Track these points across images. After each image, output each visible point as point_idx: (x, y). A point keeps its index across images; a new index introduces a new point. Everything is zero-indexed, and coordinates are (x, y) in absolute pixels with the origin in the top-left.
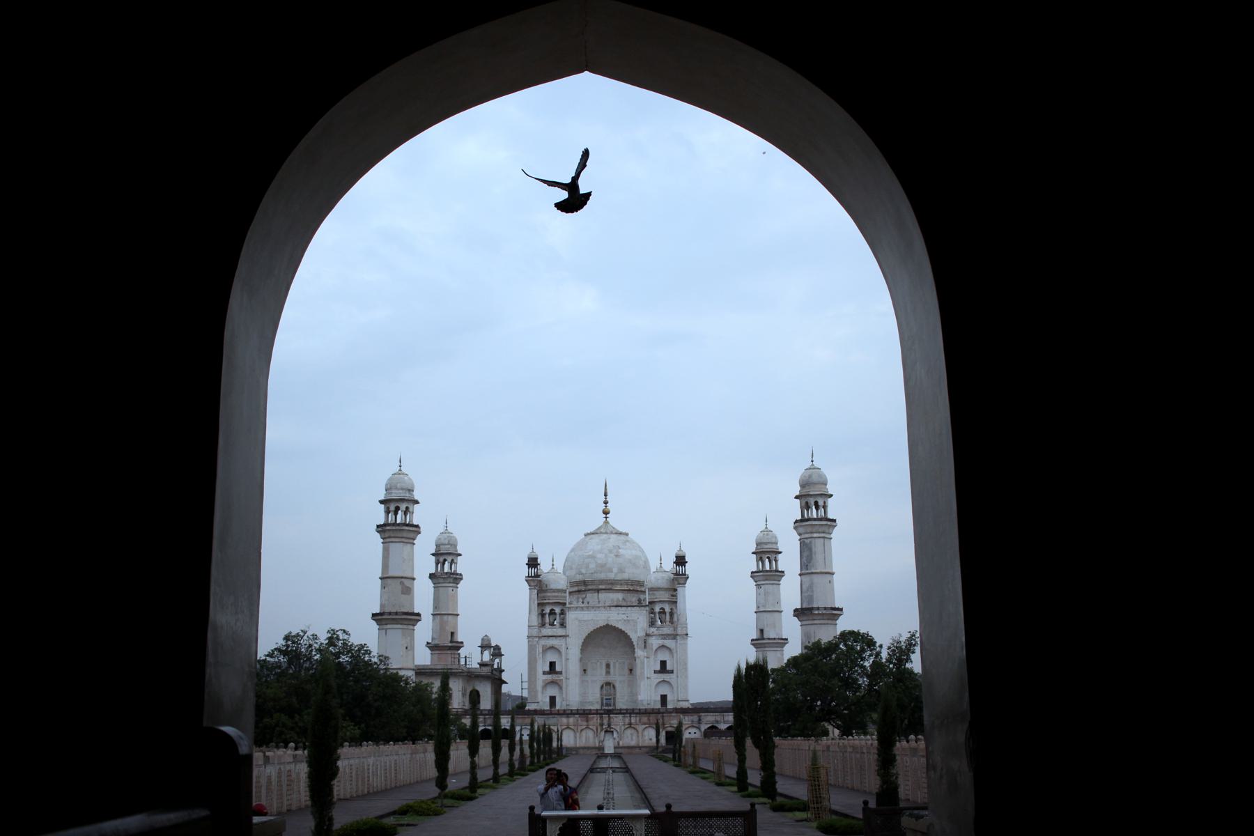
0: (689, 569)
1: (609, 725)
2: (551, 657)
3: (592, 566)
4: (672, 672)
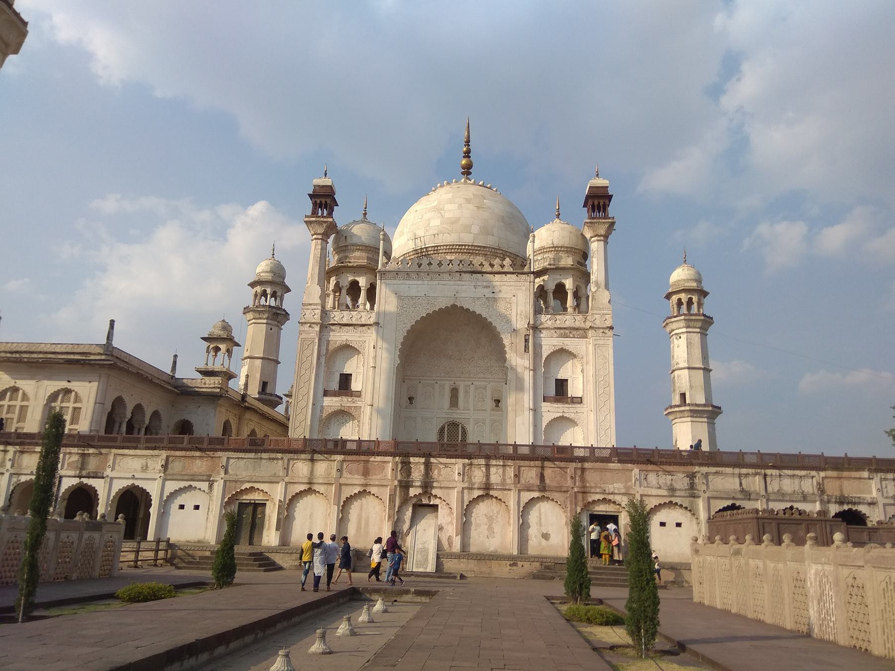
1: (427, 486)
3: (436, 222)
4: (579, 401)
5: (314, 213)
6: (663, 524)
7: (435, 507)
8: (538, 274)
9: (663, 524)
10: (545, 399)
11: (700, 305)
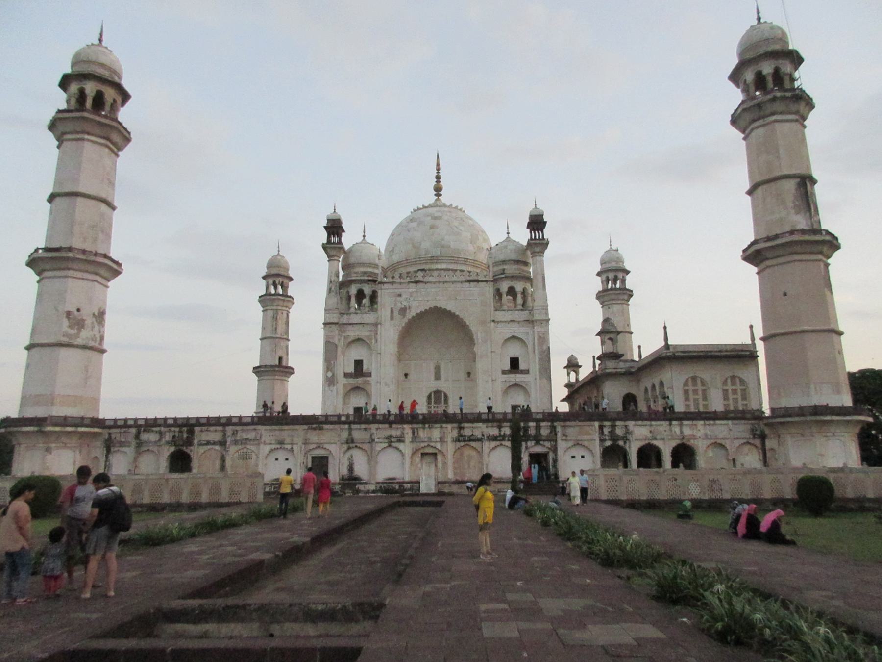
0: (547, 232)
2: (356, 353)
5: (329, 241)
6: (573, 457)
7: (435, 454)
8: (495, 281)
9: (573, 457)
10: (504, 372)
11: (623, 281)
